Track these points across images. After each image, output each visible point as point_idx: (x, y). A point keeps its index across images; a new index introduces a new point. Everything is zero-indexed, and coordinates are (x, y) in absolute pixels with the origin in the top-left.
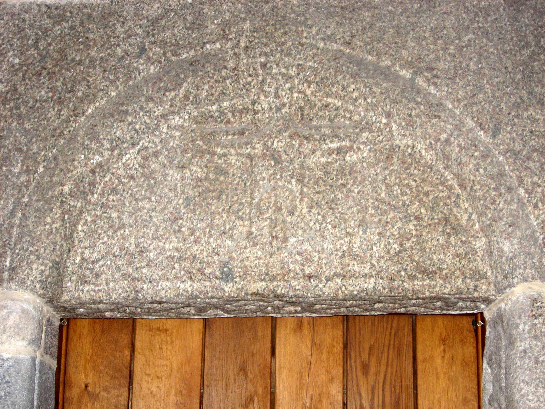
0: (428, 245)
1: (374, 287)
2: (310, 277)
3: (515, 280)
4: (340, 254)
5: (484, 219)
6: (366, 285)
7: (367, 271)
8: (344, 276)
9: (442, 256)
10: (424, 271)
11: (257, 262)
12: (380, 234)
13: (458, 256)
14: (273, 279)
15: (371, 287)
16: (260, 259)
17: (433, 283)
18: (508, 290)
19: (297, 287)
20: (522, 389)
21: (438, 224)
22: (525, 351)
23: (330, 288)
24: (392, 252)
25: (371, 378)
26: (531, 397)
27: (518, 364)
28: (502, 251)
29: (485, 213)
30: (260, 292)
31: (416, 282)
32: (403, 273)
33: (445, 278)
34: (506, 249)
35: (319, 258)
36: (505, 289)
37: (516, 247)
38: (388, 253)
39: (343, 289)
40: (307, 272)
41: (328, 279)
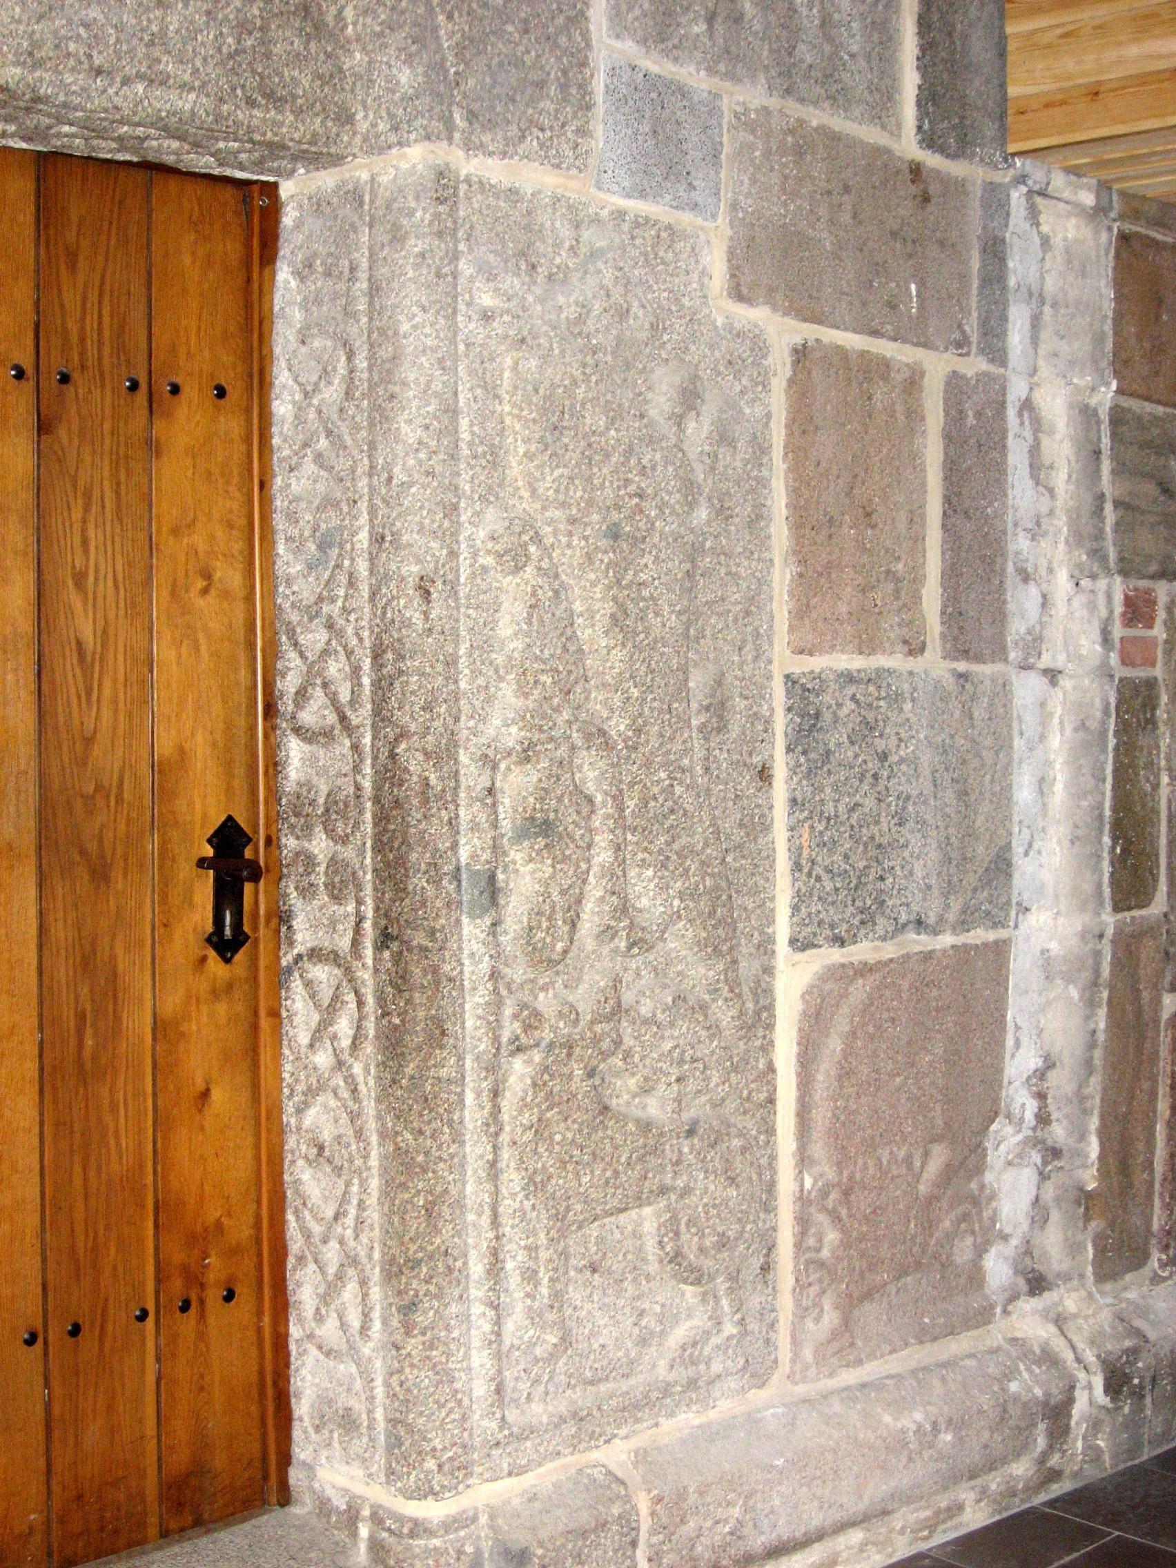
0: (277, 49)
1: (192, 110)
2: (99, 72)
3: (413, 137)
4: (147, 38)
5: (369, 20)
6: (180, 103)
7: (187, 77)
8: (152, 81)
9: (296, 73)
10: (270, 96)
11: (13, 27)
12: (208, 13)
13: (320, 77)
14: (38, 64)
15: (187, 107)
16: (19, 21)
17: (279, 117)
18: (394, 151)
19: (74, 88)
20: (414, 316)
21: (294, 13)
22: (422, 255)
23: (126, 98)
24: (225, 50)
25: (81, 278)
26: (427, 330)
27: (410, 274)
28: (398, 83)
29: (374, 12)
30: (12, 86)
31: (256, 112)
32: (239, 92)
33: (298, 112)
34: (404, 80)
35: (118, 40)
36: (390, 147)
37: (420, 79)
38: (220, 50)
39: (146, 103)
40: (97, 62)
41: (126, 81)
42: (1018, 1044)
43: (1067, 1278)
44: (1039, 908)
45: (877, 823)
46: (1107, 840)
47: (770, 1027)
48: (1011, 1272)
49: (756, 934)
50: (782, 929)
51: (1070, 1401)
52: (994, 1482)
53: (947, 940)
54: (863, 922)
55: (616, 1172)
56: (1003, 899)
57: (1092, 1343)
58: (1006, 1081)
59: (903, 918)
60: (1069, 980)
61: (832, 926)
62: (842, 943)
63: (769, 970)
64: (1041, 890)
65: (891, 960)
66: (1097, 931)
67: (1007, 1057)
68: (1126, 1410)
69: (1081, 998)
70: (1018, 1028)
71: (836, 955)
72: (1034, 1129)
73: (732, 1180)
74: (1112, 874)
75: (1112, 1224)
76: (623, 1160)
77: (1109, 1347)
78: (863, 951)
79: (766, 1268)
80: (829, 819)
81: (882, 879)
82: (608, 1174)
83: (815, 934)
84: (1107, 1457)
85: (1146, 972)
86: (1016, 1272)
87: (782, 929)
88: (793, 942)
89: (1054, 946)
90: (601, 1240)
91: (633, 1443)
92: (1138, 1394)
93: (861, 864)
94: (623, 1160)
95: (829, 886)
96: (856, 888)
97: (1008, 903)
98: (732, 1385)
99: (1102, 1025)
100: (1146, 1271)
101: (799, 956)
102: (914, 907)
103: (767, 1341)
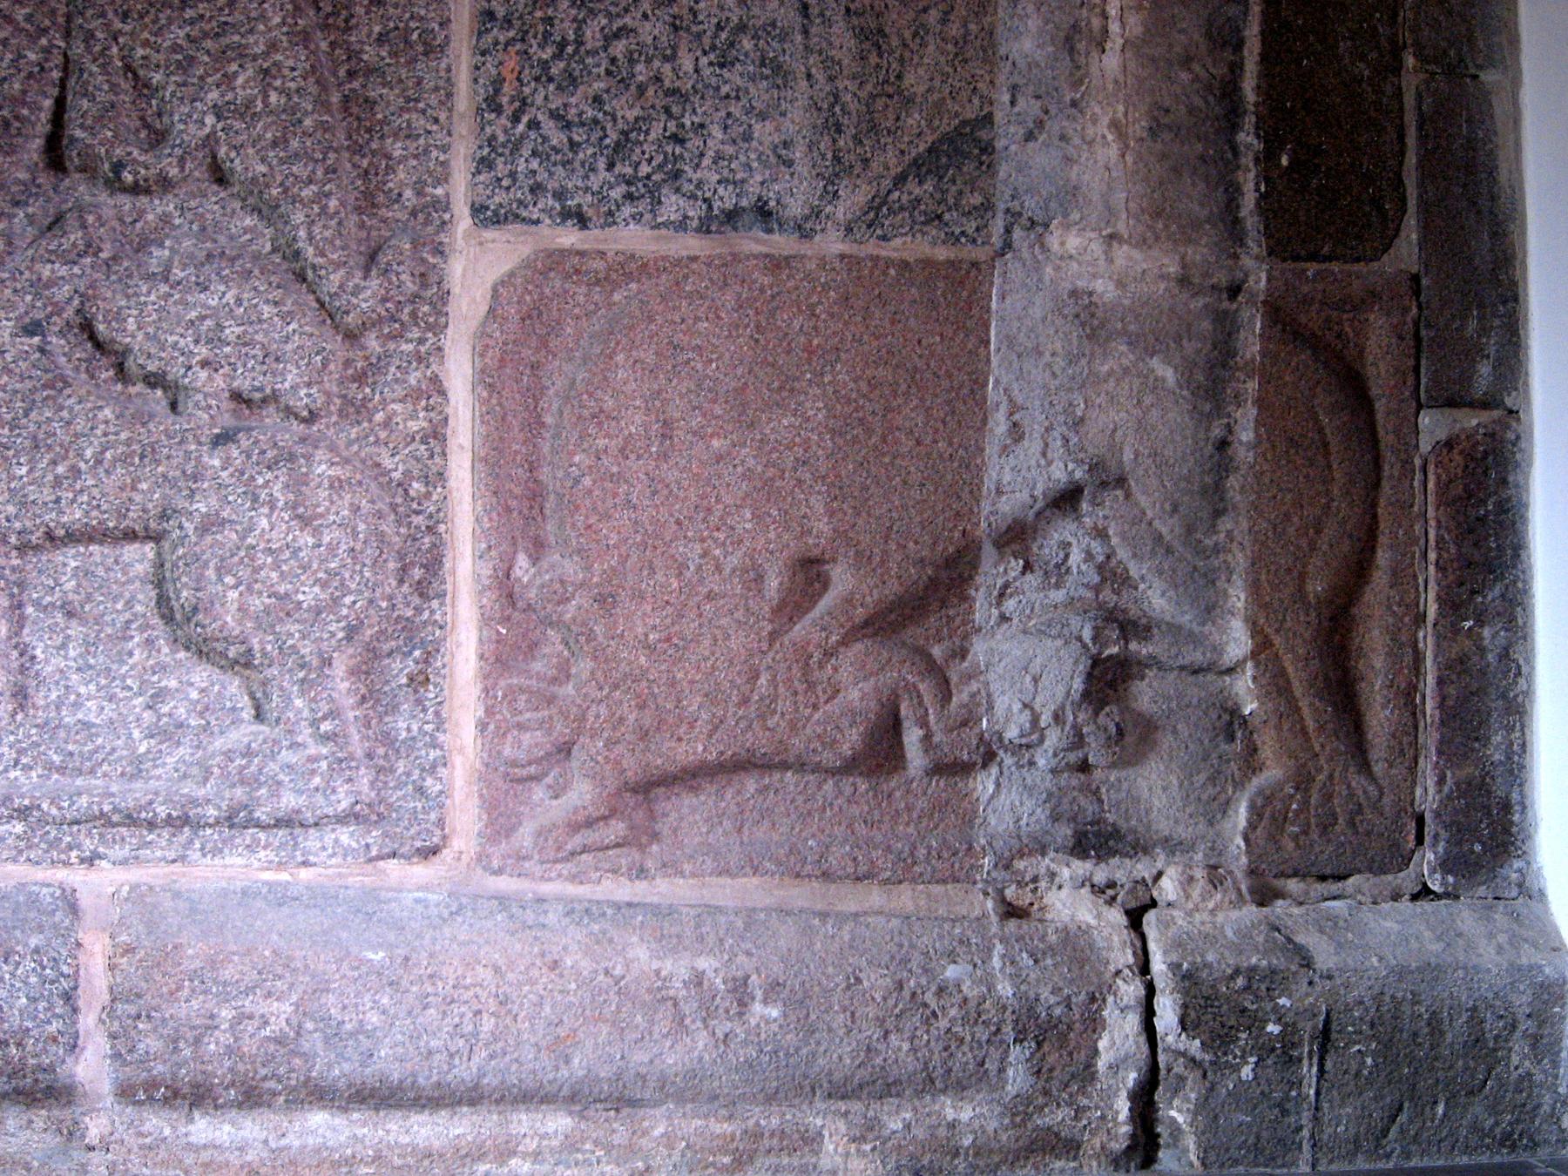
42: (1017, 432)
43: (1172, 846)
44: (1067, 227)
45: (671, 58)
46: (1247, 138)
47: (438, 328)
48: (1042, 814)
49: (408, 193)
50: (460, 189)
51: (1094, 1024)
52: (895, 1119)
53: (832, 243)
54: (629, 197)
55: (75, 472)
56: (977, 199)
57: (1178, 944)
58: (989, 484)
59: (726, 198)
60: (1146, 343)
61: (560, 195)
62: (583, 222)
63: (439, 251)
64: (1070, 195)
65: (694, 259)
66: (1221, 278)
67: (991, 450)
68: (1246, 1072)
69: (1186, 380)
70: (1014, 408)
71: (569, 237)
72: (1097, 590)
73: (305, 521)
74: (1263, 197)
75: (1302, 781)
76: (89, 453)
77: (1210, 957)
78: (631, 237)
79: (419, 681)
80: (562, 46)
81: (678, 139)
82: (60, 469)
83: (520, 203)
84: (1190, 1142)
85: (1380, 371)
86: (1055, 818)
87: (460, 189)
88: (477, 210)
89: (1104, 288)
90: (84, 573)
91: (135, 875)
92: (1283, 1053)
93: (631, 115)
94: (89, 453)
95: (557, 138)
96: (618, 146)
97: (988, 206)
98: (345, 839)
99: (1246, 435)
100: (1405, 879)
101: (489, 234)
102: (753, 188)
103: (420, 790)
